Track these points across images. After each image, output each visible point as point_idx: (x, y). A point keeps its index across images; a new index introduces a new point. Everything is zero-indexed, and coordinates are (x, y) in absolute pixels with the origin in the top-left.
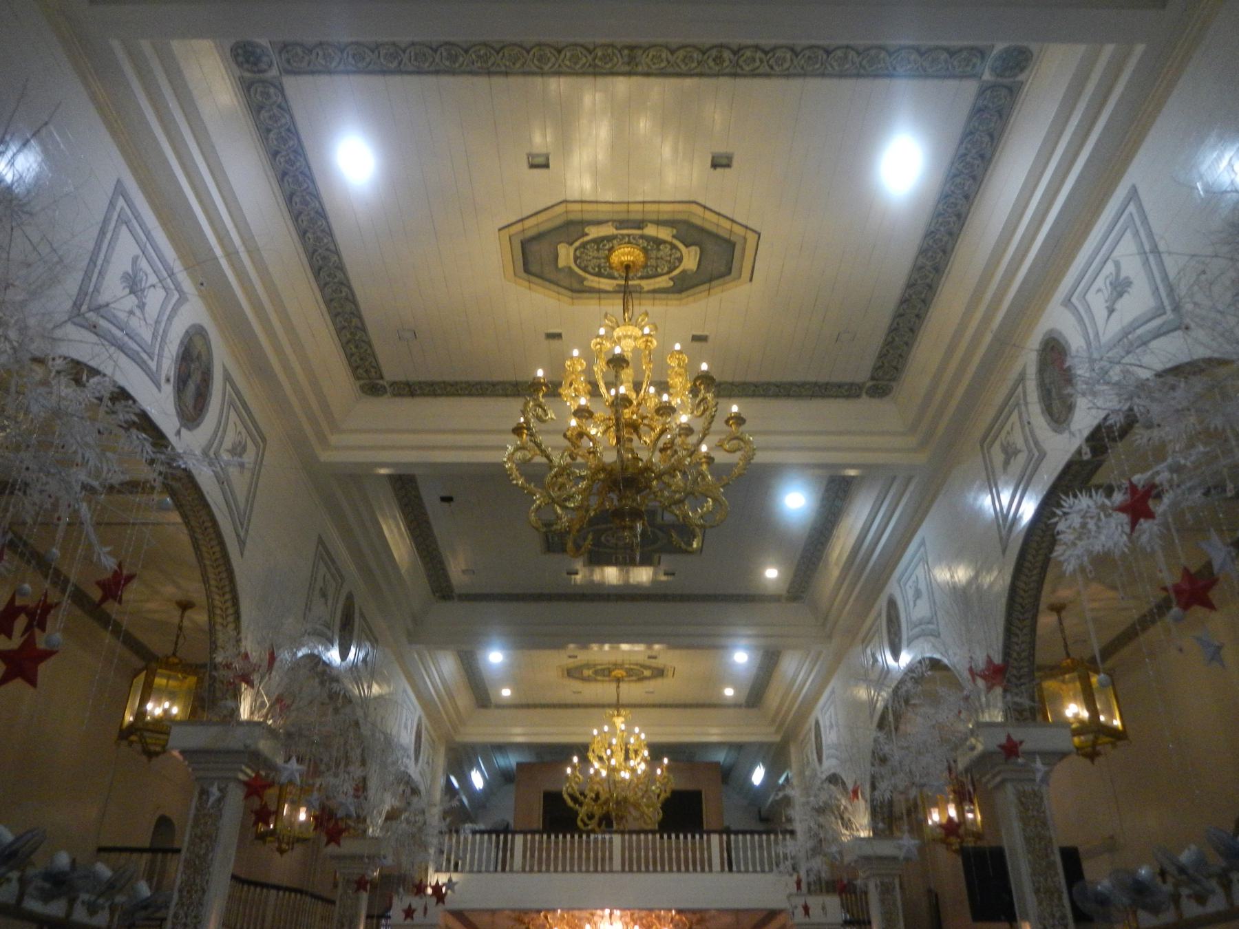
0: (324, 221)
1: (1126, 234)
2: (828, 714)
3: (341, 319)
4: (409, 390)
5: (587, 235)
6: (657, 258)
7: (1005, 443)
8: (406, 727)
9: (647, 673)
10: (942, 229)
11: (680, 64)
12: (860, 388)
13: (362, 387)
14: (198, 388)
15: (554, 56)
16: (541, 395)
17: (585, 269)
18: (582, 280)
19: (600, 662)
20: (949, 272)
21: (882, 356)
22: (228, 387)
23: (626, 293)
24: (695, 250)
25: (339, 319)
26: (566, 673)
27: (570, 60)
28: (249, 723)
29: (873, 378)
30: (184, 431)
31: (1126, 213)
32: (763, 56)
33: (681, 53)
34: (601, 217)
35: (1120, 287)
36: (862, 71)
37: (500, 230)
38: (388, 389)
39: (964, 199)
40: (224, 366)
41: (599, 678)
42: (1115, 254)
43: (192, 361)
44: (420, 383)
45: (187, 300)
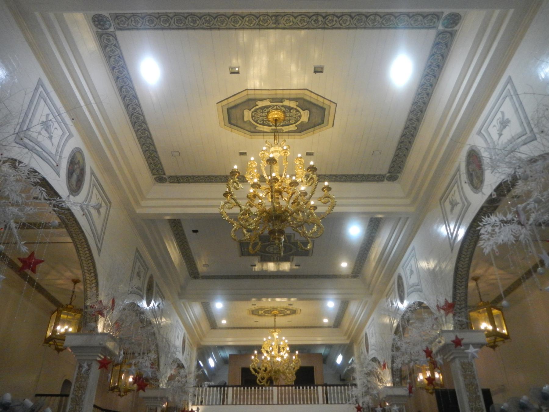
0: (136, 100)
4: (178, 180)
5: (257, 105)
6: (290, 116)
7: (451, 200)
9: (288, 312)
10: (420, 100)
11: (299, 23)
13: (155, 179)
14: (78, 176)
15: (241, 20)
16: (236, 177)
17: (256, 122)
18: (256, 127)
19: (266, 307)
20: (424, 121)
22: (93, 177)
23: (275, 132)
24: (307, 112)
25: (144, 146)
27: (248, 22)
28: (102, 334)
29: (389, 172)
30: (71, 196)
32: (337, 19)
33: (299, 18)
34: (264, 97)
35: (504, 124)
36: (383, 26)
37: (217, 103)
40: (91, 168)
41: (267, 315)
42: (501, 109)
43: (75, 164)
44: (182, 176)
45: (73, 136)
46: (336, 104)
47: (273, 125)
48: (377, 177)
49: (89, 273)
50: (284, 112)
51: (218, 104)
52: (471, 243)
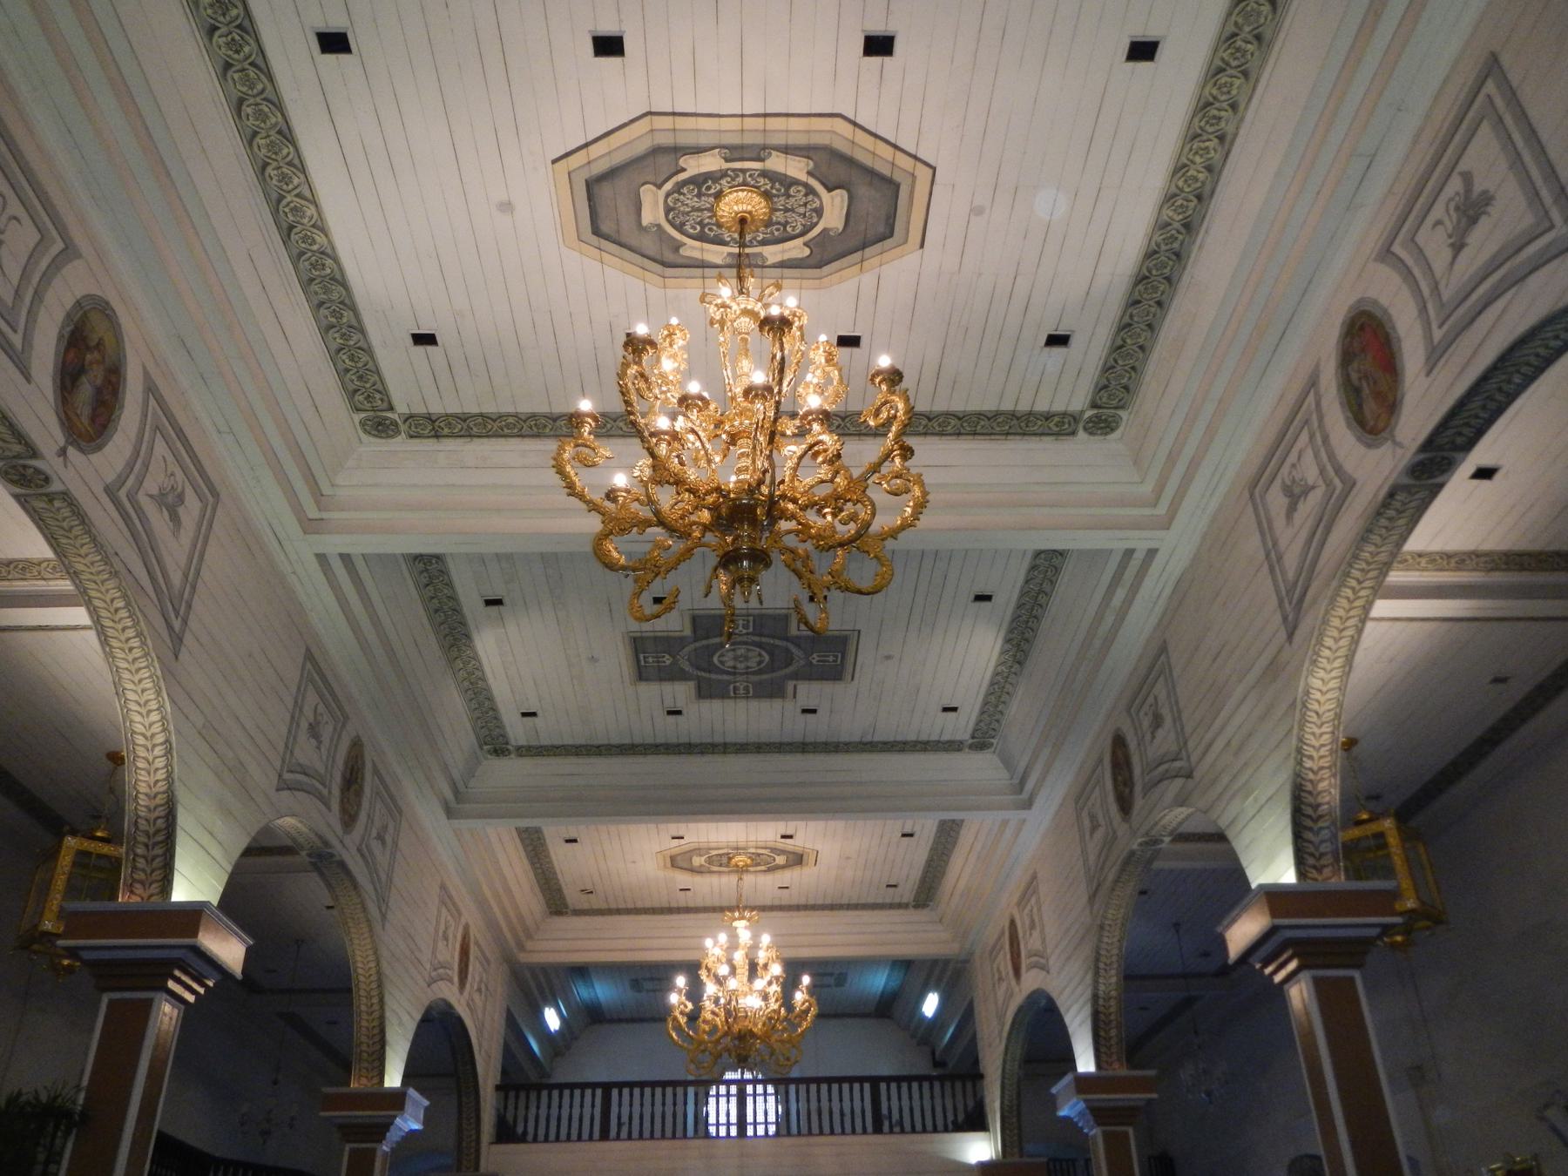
0: (291, 149)
1: (1480, 132)
2: (1029, 907)
3: (326, 312)
4: (433, 427)
5: (683, 170)
8: (446, 938)
9: (780, 860)
10: (1198, 159)
12: (1075, 419)
13: (363, 424)
14: (99, 391)
18: (677, 247)
21: (1107, 369)
22: (152, 402)
24: (840, 197)
25: (323, 312)
26: (668, 860)
29: (1094, 405)
30: (72, 452)
31: (1481, 98)
34: (704, 141)
37: (554, 162)
38: (403, 427)
39: (1230, 110)
42: (1463, 166)
43: (88, 348)
45: (78, 255)
46: (934, 169)
47: (733, 239)
48: (1056, 419)
49: (144, 711)
50: (767, 195)
51: (557, 165)
52: (1352, 613)
